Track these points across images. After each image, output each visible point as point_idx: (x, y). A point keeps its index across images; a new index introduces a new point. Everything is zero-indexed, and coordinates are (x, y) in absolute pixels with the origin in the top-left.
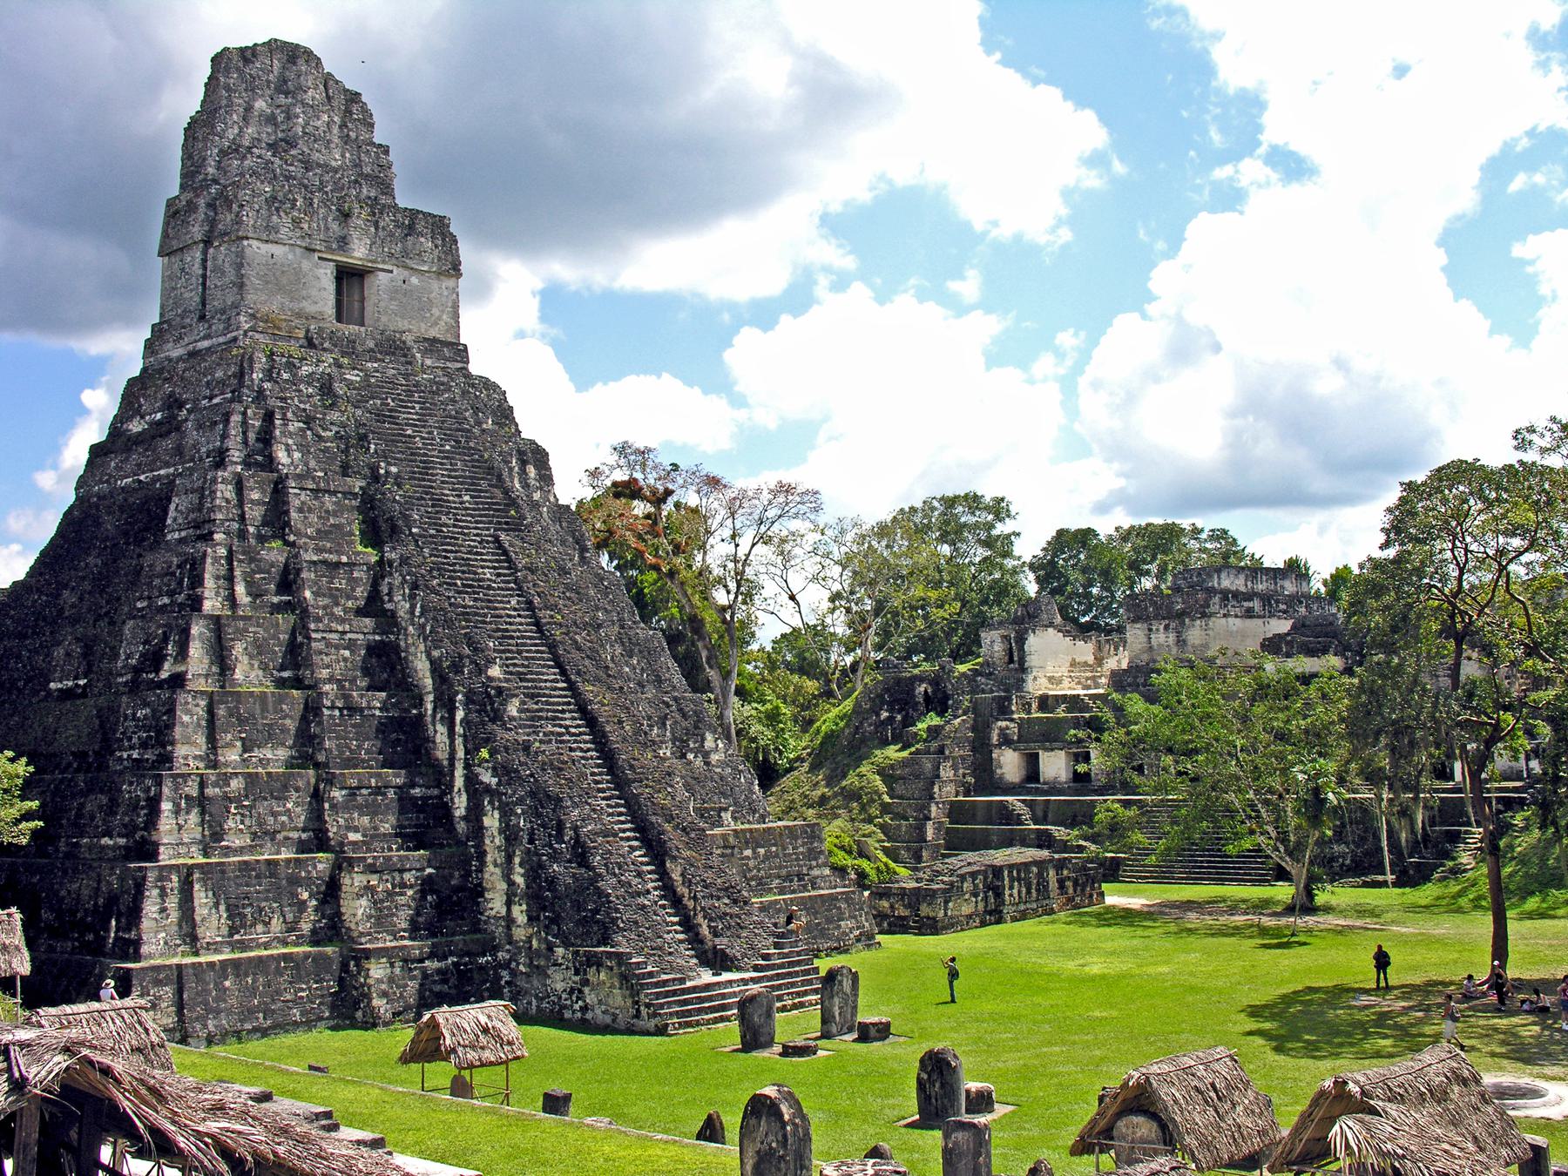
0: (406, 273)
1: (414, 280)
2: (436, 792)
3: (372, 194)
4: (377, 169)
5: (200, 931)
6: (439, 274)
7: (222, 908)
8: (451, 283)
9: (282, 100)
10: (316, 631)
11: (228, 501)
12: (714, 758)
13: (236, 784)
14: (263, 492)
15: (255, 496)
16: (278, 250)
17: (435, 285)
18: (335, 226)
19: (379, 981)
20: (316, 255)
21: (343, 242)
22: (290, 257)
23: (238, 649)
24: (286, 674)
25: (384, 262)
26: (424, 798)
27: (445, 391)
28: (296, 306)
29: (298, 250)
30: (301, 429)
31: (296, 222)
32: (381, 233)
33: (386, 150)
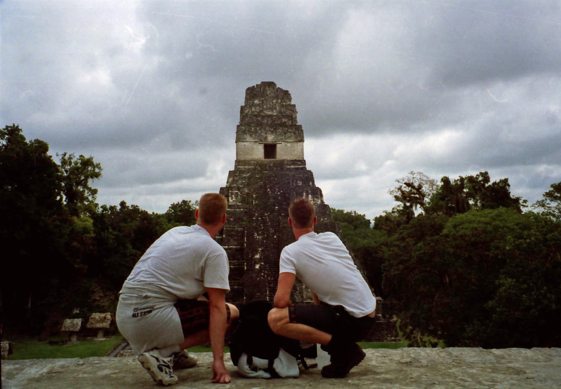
1: (289, 145)
2: (242, 287)
3: (286, 120)
6: (296, 142)
9: (261, 99)
21: (266, 138)
26: (237, 289)
31: (251, 136)
32: (278, 134)
33: (294, 106)
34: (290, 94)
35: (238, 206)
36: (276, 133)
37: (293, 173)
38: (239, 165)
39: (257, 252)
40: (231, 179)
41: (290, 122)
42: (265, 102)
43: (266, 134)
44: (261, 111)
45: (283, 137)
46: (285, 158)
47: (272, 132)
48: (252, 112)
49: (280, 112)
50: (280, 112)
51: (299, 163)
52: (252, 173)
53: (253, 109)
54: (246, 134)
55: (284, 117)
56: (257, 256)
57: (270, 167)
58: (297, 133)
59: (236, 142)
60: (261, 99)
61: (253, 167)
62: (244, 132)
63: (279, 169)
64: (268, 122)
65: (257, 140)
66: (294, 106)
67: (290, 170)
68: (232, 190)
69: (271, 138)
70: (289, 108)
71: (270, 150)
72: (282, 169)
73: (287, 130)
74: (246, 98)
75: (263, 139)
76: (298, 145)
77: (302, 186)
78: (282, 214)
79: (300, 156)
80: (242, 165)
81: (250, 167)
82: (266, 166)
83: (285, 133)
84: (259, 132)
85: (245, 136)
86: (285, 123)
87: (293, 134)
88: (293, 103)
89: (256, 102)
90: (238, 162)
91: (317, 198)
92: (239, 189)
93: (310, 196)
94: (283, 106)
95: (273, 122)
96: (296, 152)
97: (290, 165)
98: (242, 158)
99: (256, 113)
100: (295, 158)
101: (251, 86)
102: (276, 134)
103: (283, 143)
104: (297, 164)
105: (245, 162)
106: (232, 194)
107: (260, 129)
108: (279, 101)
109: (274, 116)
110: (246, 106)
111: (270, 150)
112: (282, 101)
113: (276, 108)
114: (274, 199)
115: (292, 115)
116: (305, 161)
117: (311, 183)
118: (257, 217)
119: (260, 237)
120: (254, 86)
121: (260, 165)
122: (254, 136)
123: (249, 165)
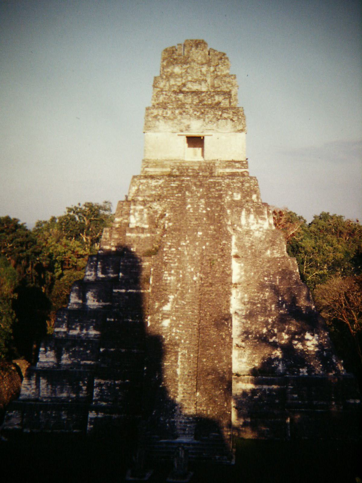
4: (229, 86)
5: (41, 394)
7: (50, 387)
10: (116, 288)
11: (106, 239)
12: (308, 343)
13: (69, 343)
14: (120, 235)
15: (116, 236)
19: (91, 419)
20: (177, 134)
23: (89, 295)
24: (108, 304)
27: (218, 186)
30: (143, 210)
32: (207, 120)
35: (143, 229)
36: (204, 121)
37: (227, 181)
38: (147, 167)
39: (167, 301)
40: (134, 189)
41: (227, 101)
42: (189, 71)
44: (184, 85)
45: (215, 125)
47: (199, 118)
48: (171, 86)
49: (213, 86)
50: (213, 86)
51: (237, 165)
52: (166, 181)
53: (172, 82)
54: (158, 120)
55: (218, 93)
56: (167, 308)
57: (193, 169)
58: (235, 119)
61: (168, 170)
63: (207, 174)
64: (192, 101)
65: (175, 130)
67: (223, 177)
68: (135, 205)
69: (196, 128)
70: (227, 80)
72: (211, 173)
73: (221, 116)
77: (240, 201)
78: (207, 244)
80: (151, 167)
81: (164, 170)
82: (187, 170)
83: (218, 120)
85: (157, 123)
86: (219, 103)
87: (229, 120)
89: (177, 70)
91: (264, 219)
92: (144, 203)
93: (252, 216)
95: (201, 102)
97: (226, 167)
98: (153, 156)
99: (175, 88)
102: (204, 121)
104: (233, 167)
105: (156, 164)
106: (135, 210)
107: (181, 114)
108: (212, 69)
109: (202, 92)
110: (161, 76)
112: (215, 70)
113: (206, 81)
114: (196, 219)
115: (230, 92)
117: (254, 197)
118: (170, 247)
119: (173, 278)
123: (163, 166)
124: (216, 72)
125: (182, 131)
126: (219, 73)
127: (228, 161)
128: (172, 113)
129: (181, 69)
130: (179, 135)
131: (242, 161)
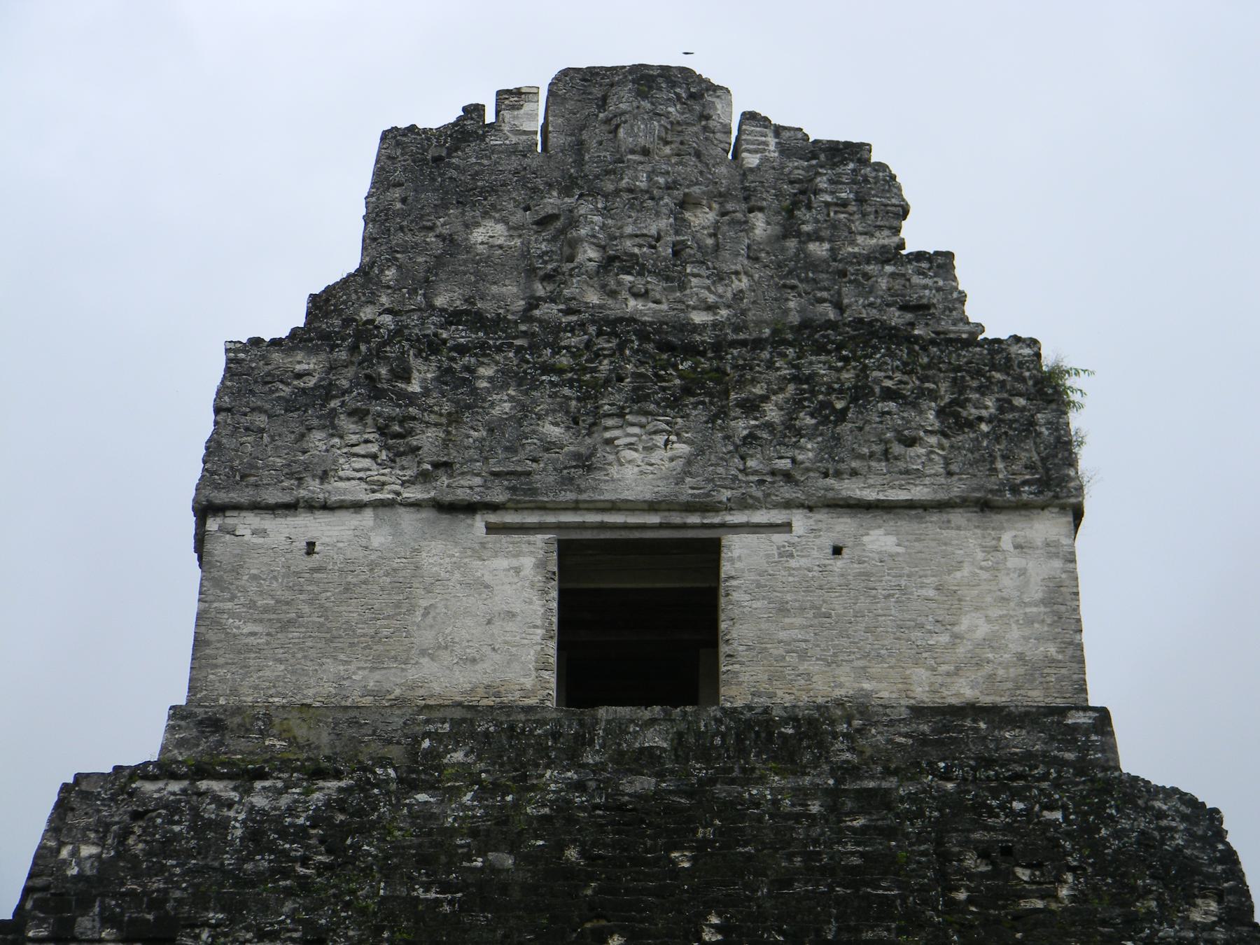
0: (843, 527)
1: (880, 539)
6: (985, 506)
8: (1045, 527)
16: (329, 530)
17: (964, 538)
18: (552, 431)
20: (479, 523)
21: (585, 463)
22: (379, 540)
25: (744, 504)
28: (394, 680)
29: (408, 520)
31: (395, 440)
33: (942, 263)
34: (882, 167)
43: (585, 419)
45: (808, 452)
46: (825, 681)
59: (204, 510)
60: (552, 202)
62: (315, 403)
65: (466, 487)
66: (942, 263)
69: (641, 469)
71: (638, 616)
74: (380, 219)
75: (544, 478)
76: (988, 564)
79: (1033, 670)
84: (503, 406)
85: (317, 440)
88: (917, 235)
89: (488, 233)
90: (204, 730)
94: (813, 264)
96: (975, 625)
98: (261, 682)
100: (964, 690)
101: (437, 113)
103: (800, 521)
108: (761, 226)
110: (364, 277)
111: (638, 616)
112: (789, 229)
116: (1103, 715)
120: (474, 111)
121: (494, 732)
122: (428, 439)
124: (792, 244)
125: (523, 493)
126: (819, 250)
127: (918, 712)
128: (445, 374)
129: (514, 229)
130: (491, 529)
131: (1062, 711)
